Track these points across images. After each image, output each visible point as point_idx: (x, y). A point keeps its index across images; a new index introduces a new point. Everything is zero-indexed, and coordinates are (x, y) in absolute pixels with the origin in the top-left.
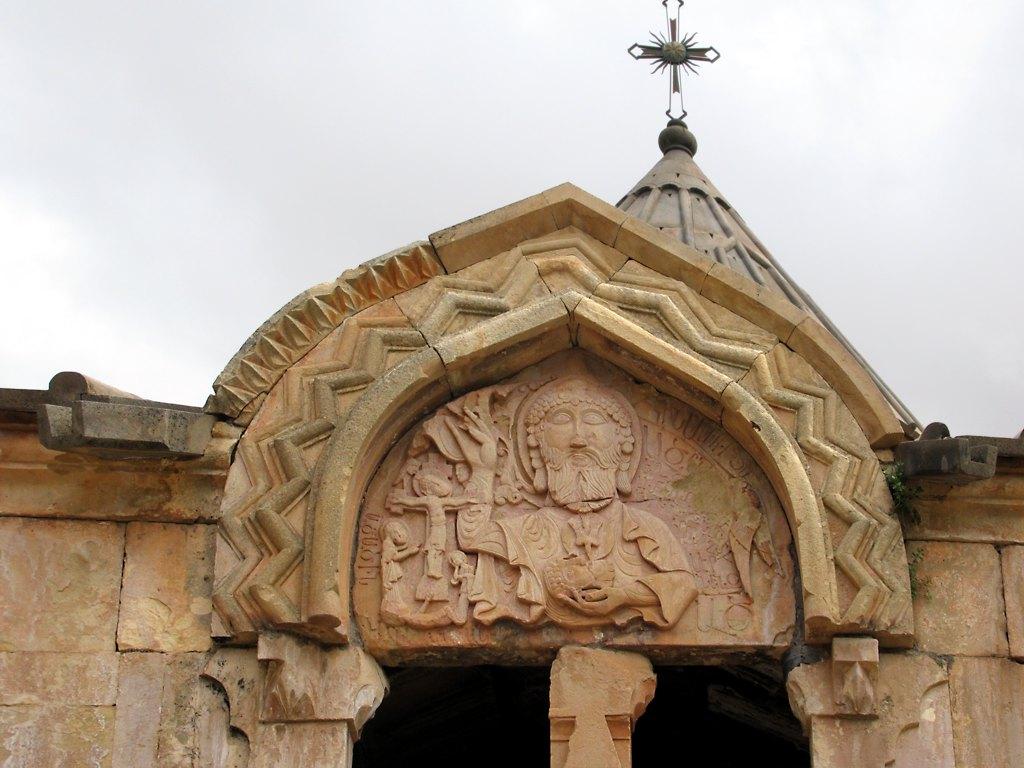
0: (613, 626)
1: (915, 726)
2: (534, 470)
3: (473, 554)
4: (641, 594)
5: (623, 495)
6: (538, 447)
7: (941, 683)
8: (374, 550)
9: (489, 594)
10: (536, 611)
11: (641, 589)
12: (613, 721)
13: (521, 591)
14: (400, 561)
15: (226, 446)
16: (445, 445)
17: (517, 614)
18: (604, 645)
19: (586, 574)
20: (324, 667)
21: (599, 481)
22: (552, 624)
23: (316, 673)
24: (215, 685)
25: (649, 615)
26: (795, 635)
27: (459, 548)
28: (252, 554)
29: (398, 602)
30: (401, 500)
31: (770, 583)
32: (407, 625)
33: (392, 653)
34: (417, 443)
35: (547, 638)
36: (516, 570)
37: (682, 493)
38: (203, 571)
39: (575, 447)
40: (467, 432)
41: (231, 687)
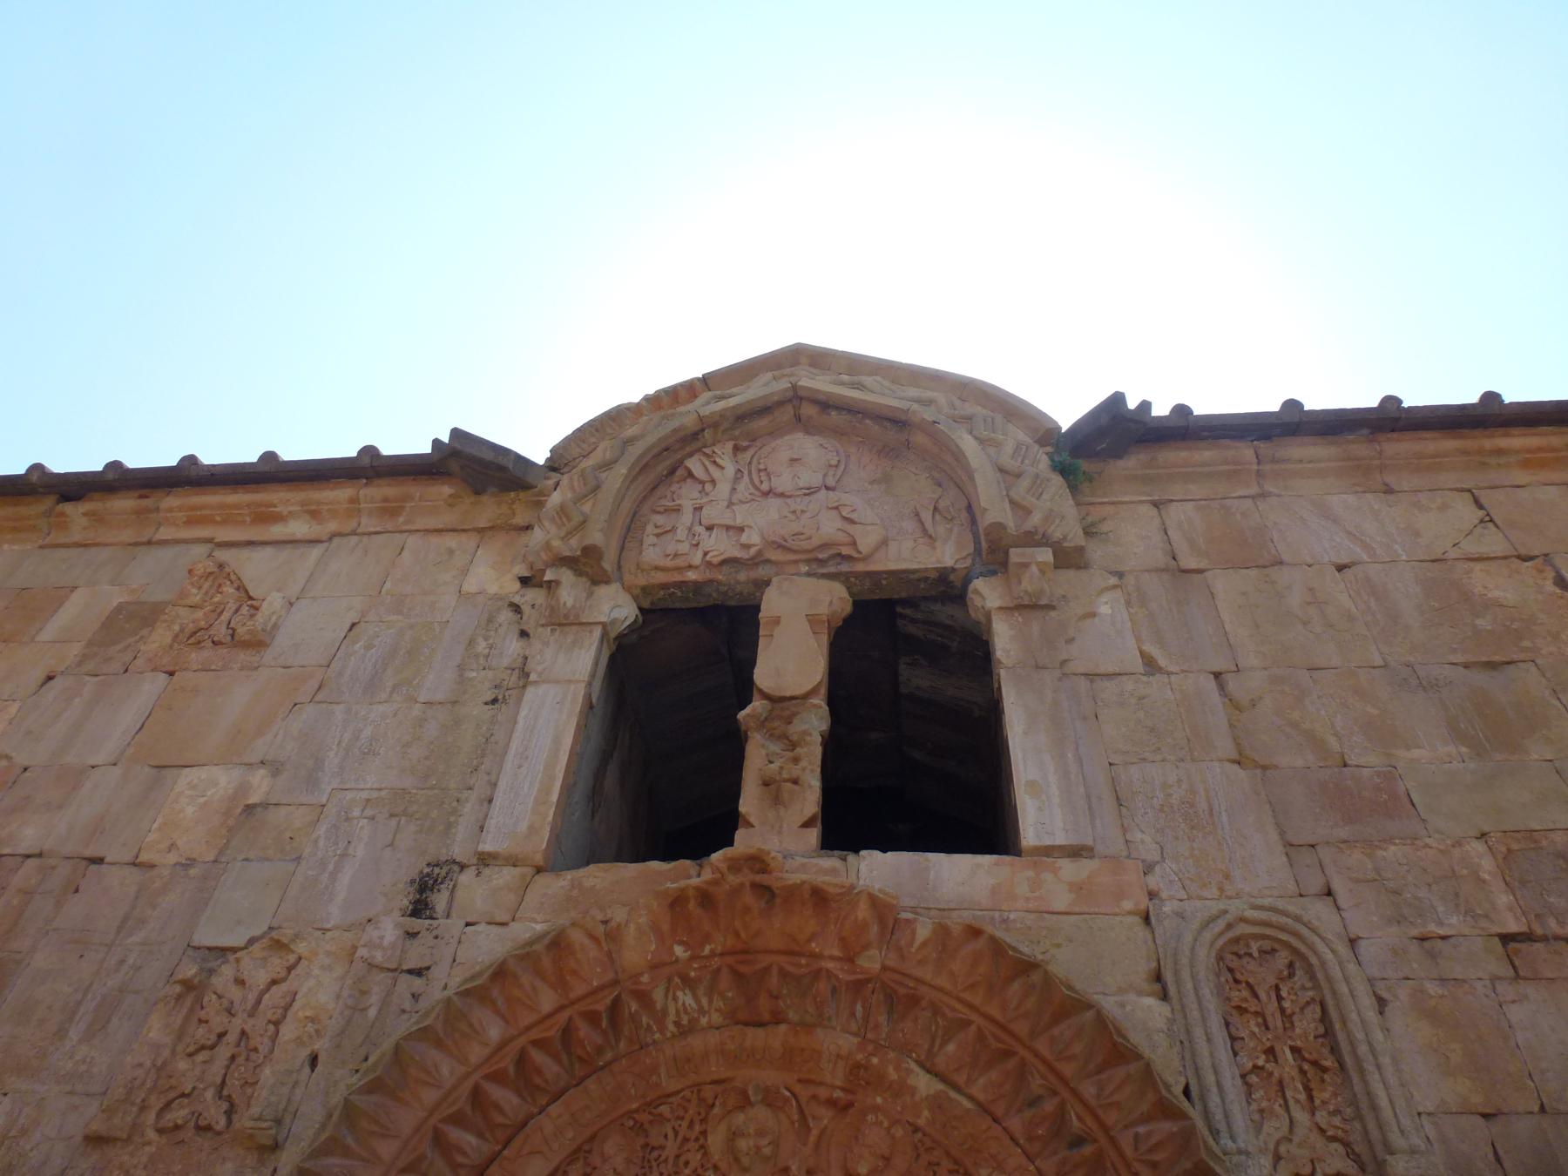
1: (1093, 615)
2: (762, 482)
3: (710, 528)
4: (841, 537)
5: (827, 488)
6: (766, 469)
7: (1115, 587)
8: (641, 532)
9: (719, 546)
10: (753, 551)
11: (840, 533)
12: (813, 620)
13: (744, 539)
14: (658, 535)
15: (551, 482)
16: (698, 471)
17: (737, 553)
18: (809, 574)
19: (795, 527)
20: (590, 595)
21: (809, 477)
22: (767, 561)
23: (584, 595)
24: (516, 608)
25: (845, 551)
26: (973, 560)
27: (701, 524)
30: (663, 504)
32: (657, 568)
33: (644, 589)
34: (680, 472)
35: (762, 572)
36: (741, 529)
39: (793, 460)
40: (715, 462)
41: (526, 609)
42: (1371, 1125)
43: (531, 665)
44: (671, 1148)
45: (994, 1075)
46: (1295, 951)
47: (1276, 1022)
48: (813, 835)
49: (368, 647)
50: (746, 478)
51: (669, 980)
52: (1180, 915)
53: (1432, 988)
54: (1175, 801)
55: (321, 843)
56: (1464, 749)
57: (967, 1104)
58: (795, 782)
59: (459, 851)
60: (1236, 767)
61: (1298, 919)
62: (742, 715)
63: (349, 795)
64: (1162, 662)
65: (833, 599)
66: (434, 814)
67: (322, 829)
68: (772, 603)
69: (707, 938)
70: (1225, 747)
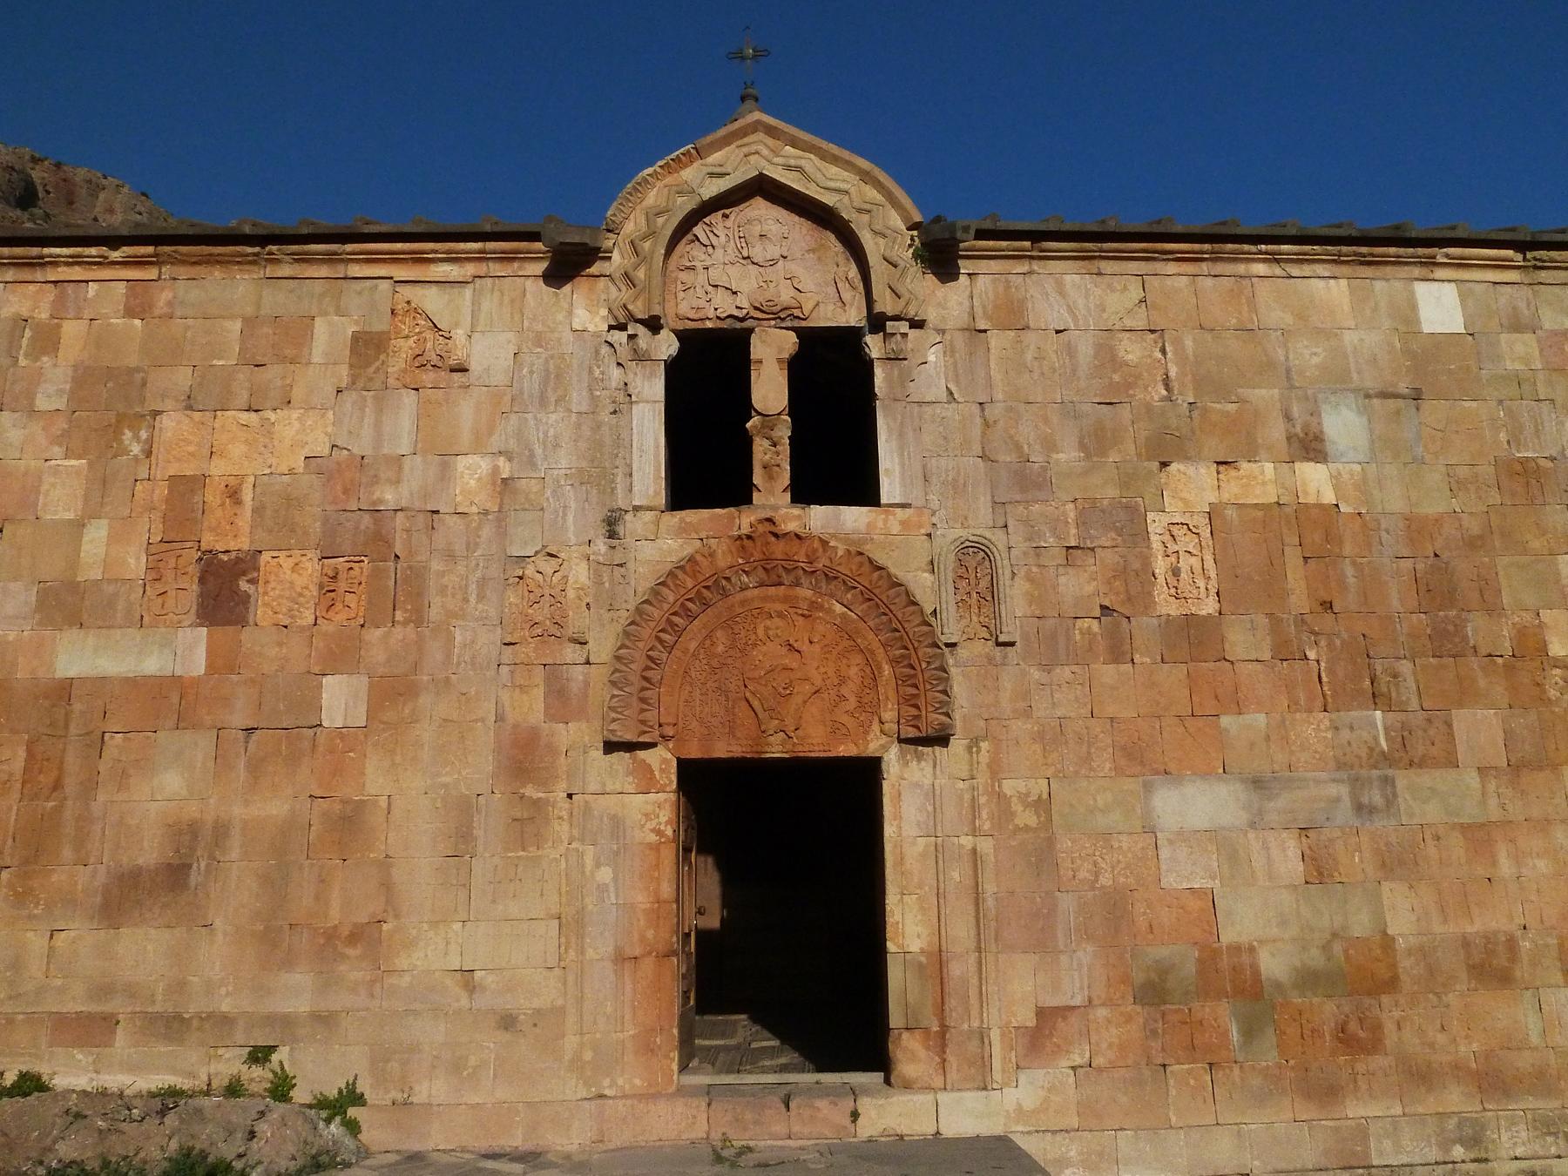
0: (780, 318)
4: (793, 303)
10: (745, 311)
12: (780, 361)
17: (736, 313)
21: (773, 251)
22: (752, 318)
25: (797, 312)
28: (624, 288)
29: (684, 309)
34: (689, 237)
35: (749, 324)
38: (603, 297)
42: (998, 623)
43: (631, 390)
45: (865, 606)
46: (986, 553)
47: (973, 582)
48: (788, 496)
49: (531, 372)
50: (732, 241)
51: (737, 571)
52: (944, 536)
53: (1035, 569)
54: (950, 479)
55: (551, 500)
56: (1082, 455)
57: (855, 617)
58: (778, 466)
59: (621, 503)
61: (989, 540)
62: (748, 425)
63: (556, 472)
64: (956, 396)
65: (788, 342)
66: (603, 482)
67: (548, 493)
68: (757, 348)
69: (752, 555)
70: (977, 449)
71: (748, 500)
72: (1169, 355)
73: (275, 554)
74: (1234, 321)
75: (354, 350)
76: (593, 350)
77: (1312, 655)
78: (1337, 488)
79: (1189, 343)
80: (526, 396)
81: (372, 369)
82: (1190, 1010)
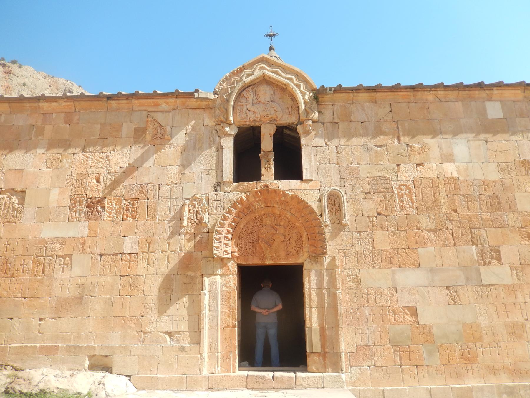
9: (251, 116)
10: (259, 119)
12: (270, 135)
16: (245, 95)
24: (216, 130)
31: (294, 113)
37: (281, 100)
38: (214, 115)
44: (258, 222)
47: (334, 205)
60: (336, 165)
62: (260, 155)
63: (199, 171)
71: (260, 179)
72: (400, 129)
73: (110, 198)
74: (422, 117)
75: (135, 133)
76: (210, 132)
77: (450, 227)
78: (458, 171)
79: (406, 124)
80: (189, 147)
81: (141, 139)
82: (409, 347)
